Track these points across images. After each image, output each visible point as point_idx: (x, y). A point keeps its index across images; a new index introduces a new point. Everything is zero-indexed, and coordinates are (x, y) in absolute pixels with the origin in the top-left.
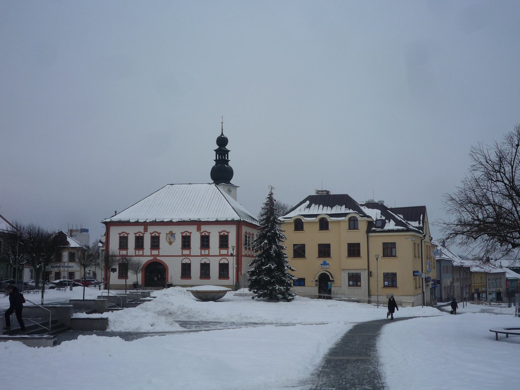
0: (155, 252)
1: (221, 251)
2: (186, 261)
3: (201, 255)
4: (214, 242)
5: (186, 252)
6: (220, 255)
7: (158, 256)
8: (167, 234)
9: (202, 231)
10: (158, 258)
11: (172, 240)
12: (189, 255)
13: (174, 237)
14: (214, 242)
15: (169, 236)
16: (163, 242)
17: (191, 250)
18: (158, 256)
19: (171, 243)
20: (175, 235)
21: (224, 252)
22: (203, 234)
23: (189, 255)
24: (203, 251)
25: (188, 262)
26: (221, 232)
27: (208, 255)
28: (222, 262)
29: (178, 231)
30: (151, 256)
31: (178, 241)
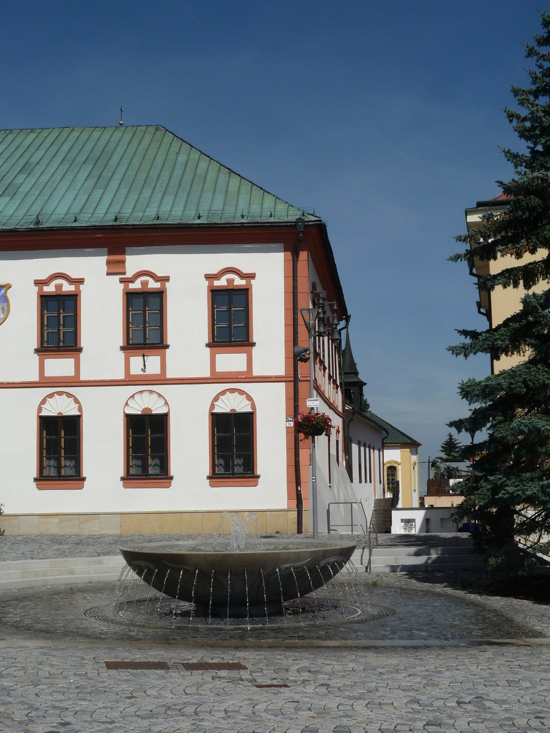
1: (219, 357)
2: (60, 406)
3: (130, 381)
4: (188, 318)
5: (59, 366)
6: (216, 378)
9: (129, 274)
14: (188, 318)
17: (82, 355)
20: (10, 294)
21: (231, 361)
22: (136, 285)
23: (75, 382)
24: (136, 362)
25: (70, 410)
26: (217, 277)
27: (161, 380)
28: (222, 407)
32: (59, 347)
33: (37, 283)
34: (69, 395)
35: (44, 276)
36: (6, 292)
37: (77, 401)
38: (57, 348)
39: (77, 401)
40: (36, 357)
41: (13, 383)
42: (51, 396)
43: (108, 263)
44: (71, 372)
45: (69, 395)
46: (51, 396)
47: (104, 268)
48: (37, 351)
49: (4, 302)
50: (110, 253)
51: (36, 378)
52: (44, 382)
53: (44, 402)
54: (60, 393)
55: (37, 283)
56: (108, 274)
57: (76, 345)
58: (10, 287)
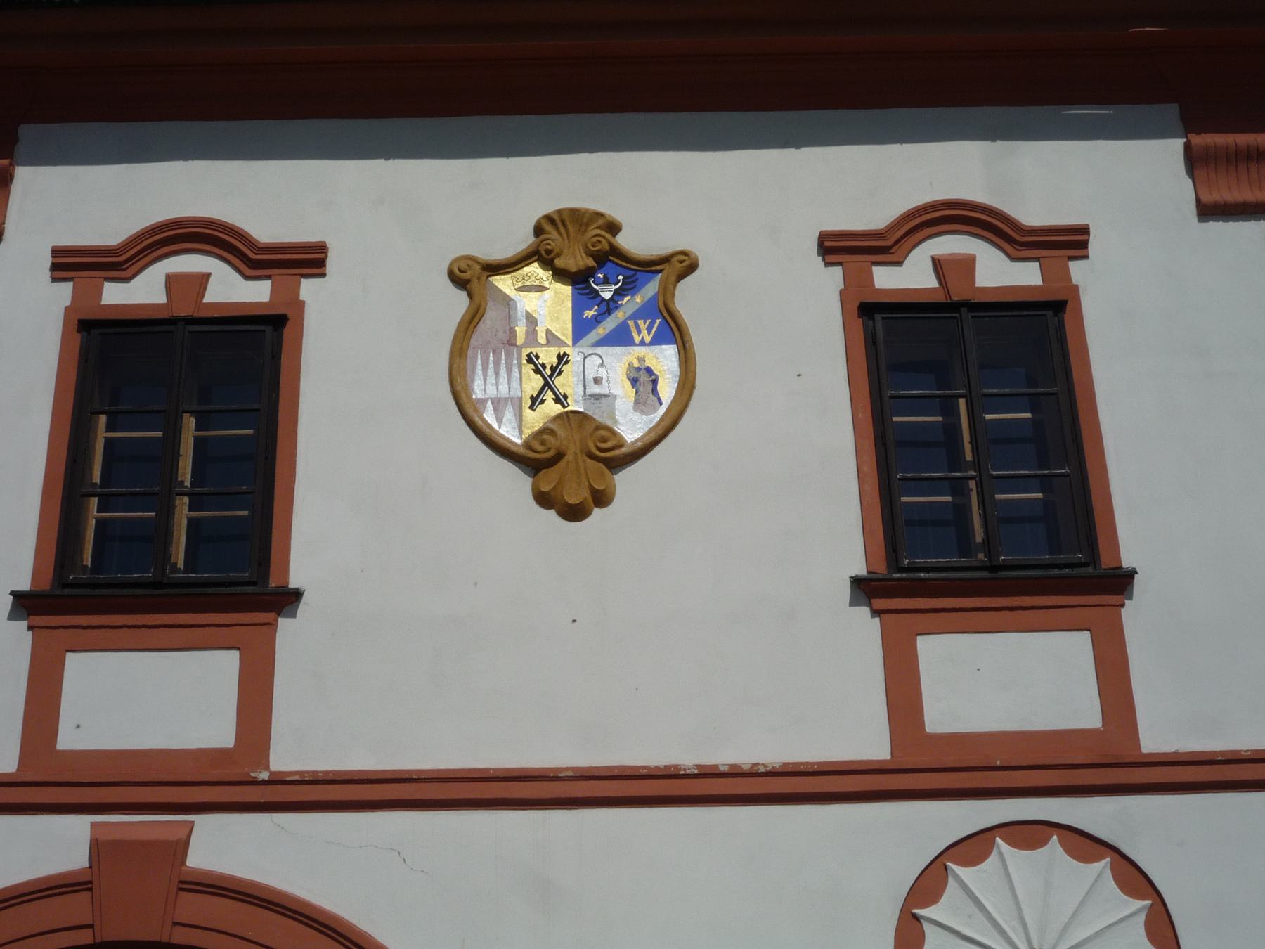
0: (151, 696)
5: (1006, 678)
7: (239, 781)
8: (471, 276)
10: (225, 845)
11: (611, 381)
12: (1110, 762)
13: (672, 329)
15: (544, 303)
16: (375, 467)
18: (239, 781)
19: (571, 469)
23: (1110, 762)
29: (764, 224)
30: (45, 784)
31: (770, 439)
32: (993, 568)
33: (834, 247)
34: (1085, 844)
35: (874, 215)
36: (667, 292)
37: (1133, 878)
38: (985, 574)
39: (1133, 878)
40: (864, 629)
41: (735, 773)
42: (972, 847)
43: (1193, 161)
44: (1083, 712)
45: (1085, 844)
46: (972, 847)
47: (1183, 191)
48: (865, 589)
49: (657, 341)
50: (1190, 124)
51: (870, 741)
52: (921, 768)
53: (928, 885)
54: (1028, 834)
55: (834, 247)
56: (1207, 211)
57: (1094, 557)
58: (692, 267)
